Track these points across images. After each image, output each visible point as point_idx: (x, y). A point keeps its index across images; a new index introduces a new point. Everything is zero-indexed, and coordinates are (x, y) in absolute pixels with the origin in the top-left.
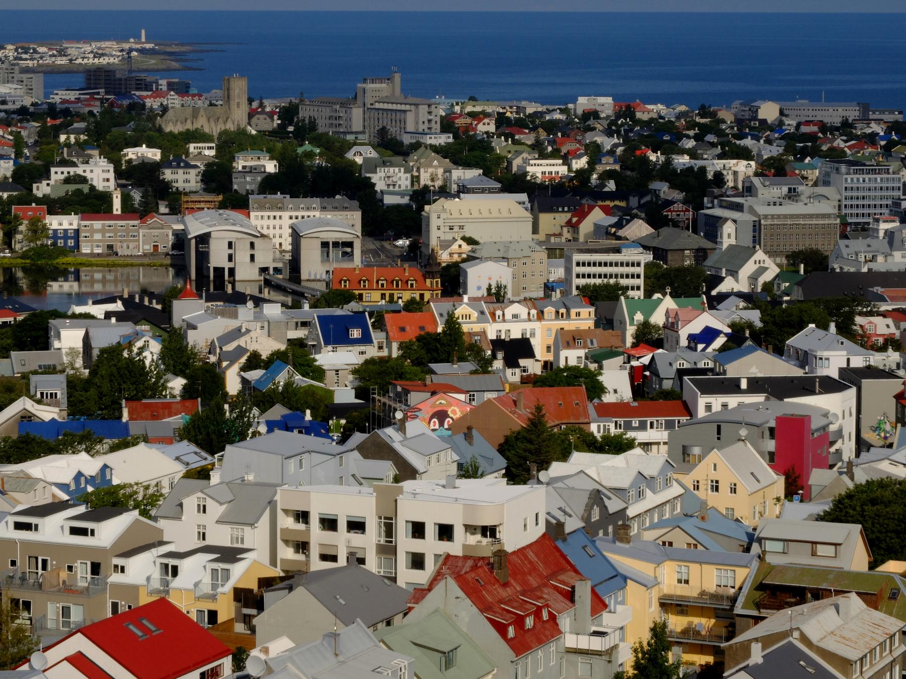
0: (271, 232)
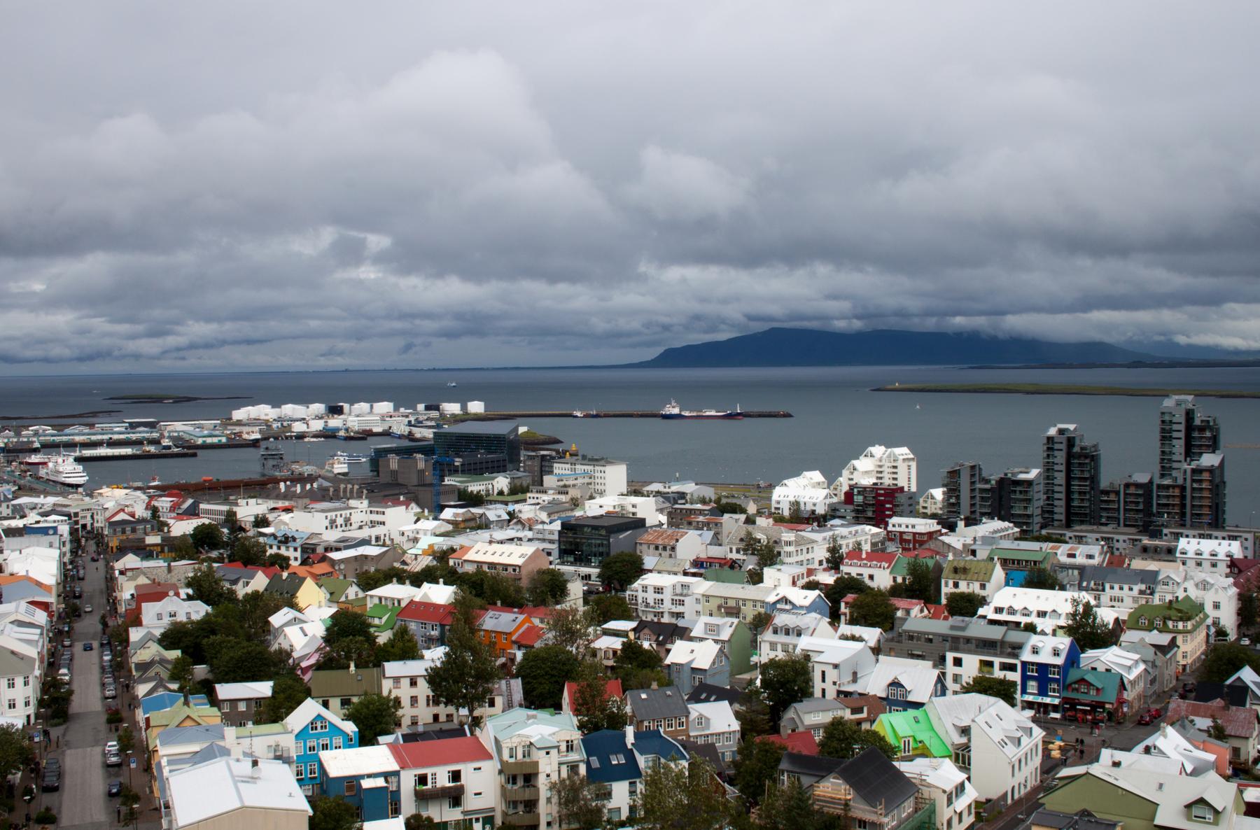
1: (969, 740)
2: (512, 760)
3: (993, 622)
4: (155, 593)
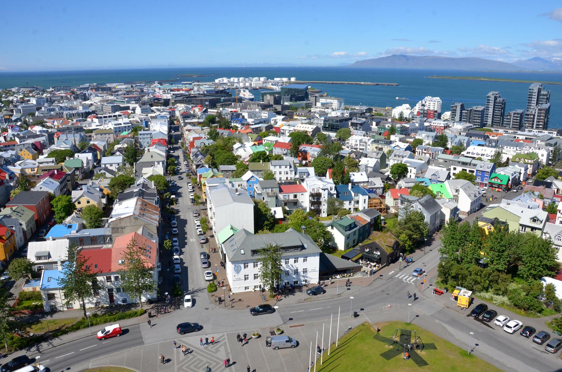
1: (459, 194)
3: (466, 157)
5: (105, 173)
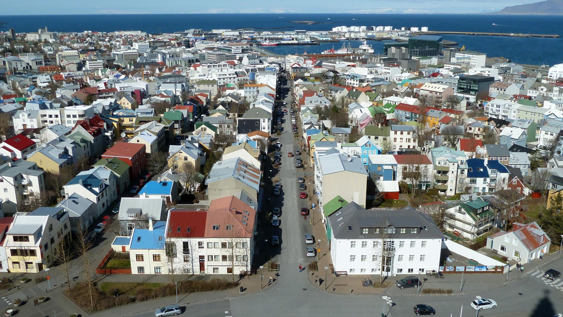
0: (24, 60)
2: (440, 165)
4: (308, 93)
5: (205, 129)
